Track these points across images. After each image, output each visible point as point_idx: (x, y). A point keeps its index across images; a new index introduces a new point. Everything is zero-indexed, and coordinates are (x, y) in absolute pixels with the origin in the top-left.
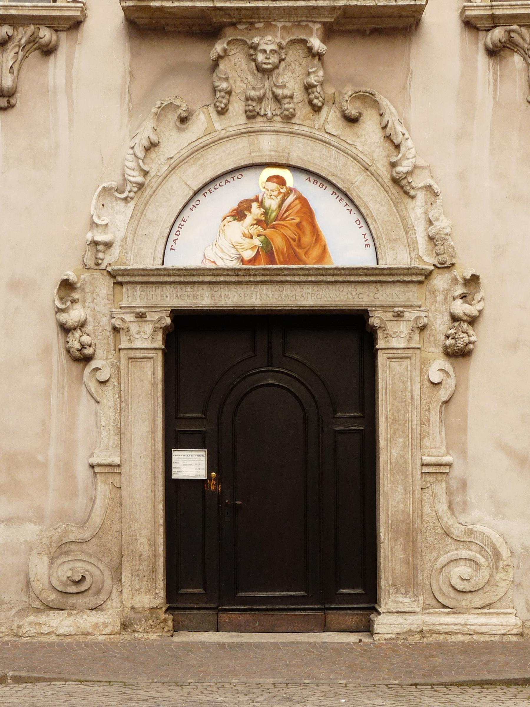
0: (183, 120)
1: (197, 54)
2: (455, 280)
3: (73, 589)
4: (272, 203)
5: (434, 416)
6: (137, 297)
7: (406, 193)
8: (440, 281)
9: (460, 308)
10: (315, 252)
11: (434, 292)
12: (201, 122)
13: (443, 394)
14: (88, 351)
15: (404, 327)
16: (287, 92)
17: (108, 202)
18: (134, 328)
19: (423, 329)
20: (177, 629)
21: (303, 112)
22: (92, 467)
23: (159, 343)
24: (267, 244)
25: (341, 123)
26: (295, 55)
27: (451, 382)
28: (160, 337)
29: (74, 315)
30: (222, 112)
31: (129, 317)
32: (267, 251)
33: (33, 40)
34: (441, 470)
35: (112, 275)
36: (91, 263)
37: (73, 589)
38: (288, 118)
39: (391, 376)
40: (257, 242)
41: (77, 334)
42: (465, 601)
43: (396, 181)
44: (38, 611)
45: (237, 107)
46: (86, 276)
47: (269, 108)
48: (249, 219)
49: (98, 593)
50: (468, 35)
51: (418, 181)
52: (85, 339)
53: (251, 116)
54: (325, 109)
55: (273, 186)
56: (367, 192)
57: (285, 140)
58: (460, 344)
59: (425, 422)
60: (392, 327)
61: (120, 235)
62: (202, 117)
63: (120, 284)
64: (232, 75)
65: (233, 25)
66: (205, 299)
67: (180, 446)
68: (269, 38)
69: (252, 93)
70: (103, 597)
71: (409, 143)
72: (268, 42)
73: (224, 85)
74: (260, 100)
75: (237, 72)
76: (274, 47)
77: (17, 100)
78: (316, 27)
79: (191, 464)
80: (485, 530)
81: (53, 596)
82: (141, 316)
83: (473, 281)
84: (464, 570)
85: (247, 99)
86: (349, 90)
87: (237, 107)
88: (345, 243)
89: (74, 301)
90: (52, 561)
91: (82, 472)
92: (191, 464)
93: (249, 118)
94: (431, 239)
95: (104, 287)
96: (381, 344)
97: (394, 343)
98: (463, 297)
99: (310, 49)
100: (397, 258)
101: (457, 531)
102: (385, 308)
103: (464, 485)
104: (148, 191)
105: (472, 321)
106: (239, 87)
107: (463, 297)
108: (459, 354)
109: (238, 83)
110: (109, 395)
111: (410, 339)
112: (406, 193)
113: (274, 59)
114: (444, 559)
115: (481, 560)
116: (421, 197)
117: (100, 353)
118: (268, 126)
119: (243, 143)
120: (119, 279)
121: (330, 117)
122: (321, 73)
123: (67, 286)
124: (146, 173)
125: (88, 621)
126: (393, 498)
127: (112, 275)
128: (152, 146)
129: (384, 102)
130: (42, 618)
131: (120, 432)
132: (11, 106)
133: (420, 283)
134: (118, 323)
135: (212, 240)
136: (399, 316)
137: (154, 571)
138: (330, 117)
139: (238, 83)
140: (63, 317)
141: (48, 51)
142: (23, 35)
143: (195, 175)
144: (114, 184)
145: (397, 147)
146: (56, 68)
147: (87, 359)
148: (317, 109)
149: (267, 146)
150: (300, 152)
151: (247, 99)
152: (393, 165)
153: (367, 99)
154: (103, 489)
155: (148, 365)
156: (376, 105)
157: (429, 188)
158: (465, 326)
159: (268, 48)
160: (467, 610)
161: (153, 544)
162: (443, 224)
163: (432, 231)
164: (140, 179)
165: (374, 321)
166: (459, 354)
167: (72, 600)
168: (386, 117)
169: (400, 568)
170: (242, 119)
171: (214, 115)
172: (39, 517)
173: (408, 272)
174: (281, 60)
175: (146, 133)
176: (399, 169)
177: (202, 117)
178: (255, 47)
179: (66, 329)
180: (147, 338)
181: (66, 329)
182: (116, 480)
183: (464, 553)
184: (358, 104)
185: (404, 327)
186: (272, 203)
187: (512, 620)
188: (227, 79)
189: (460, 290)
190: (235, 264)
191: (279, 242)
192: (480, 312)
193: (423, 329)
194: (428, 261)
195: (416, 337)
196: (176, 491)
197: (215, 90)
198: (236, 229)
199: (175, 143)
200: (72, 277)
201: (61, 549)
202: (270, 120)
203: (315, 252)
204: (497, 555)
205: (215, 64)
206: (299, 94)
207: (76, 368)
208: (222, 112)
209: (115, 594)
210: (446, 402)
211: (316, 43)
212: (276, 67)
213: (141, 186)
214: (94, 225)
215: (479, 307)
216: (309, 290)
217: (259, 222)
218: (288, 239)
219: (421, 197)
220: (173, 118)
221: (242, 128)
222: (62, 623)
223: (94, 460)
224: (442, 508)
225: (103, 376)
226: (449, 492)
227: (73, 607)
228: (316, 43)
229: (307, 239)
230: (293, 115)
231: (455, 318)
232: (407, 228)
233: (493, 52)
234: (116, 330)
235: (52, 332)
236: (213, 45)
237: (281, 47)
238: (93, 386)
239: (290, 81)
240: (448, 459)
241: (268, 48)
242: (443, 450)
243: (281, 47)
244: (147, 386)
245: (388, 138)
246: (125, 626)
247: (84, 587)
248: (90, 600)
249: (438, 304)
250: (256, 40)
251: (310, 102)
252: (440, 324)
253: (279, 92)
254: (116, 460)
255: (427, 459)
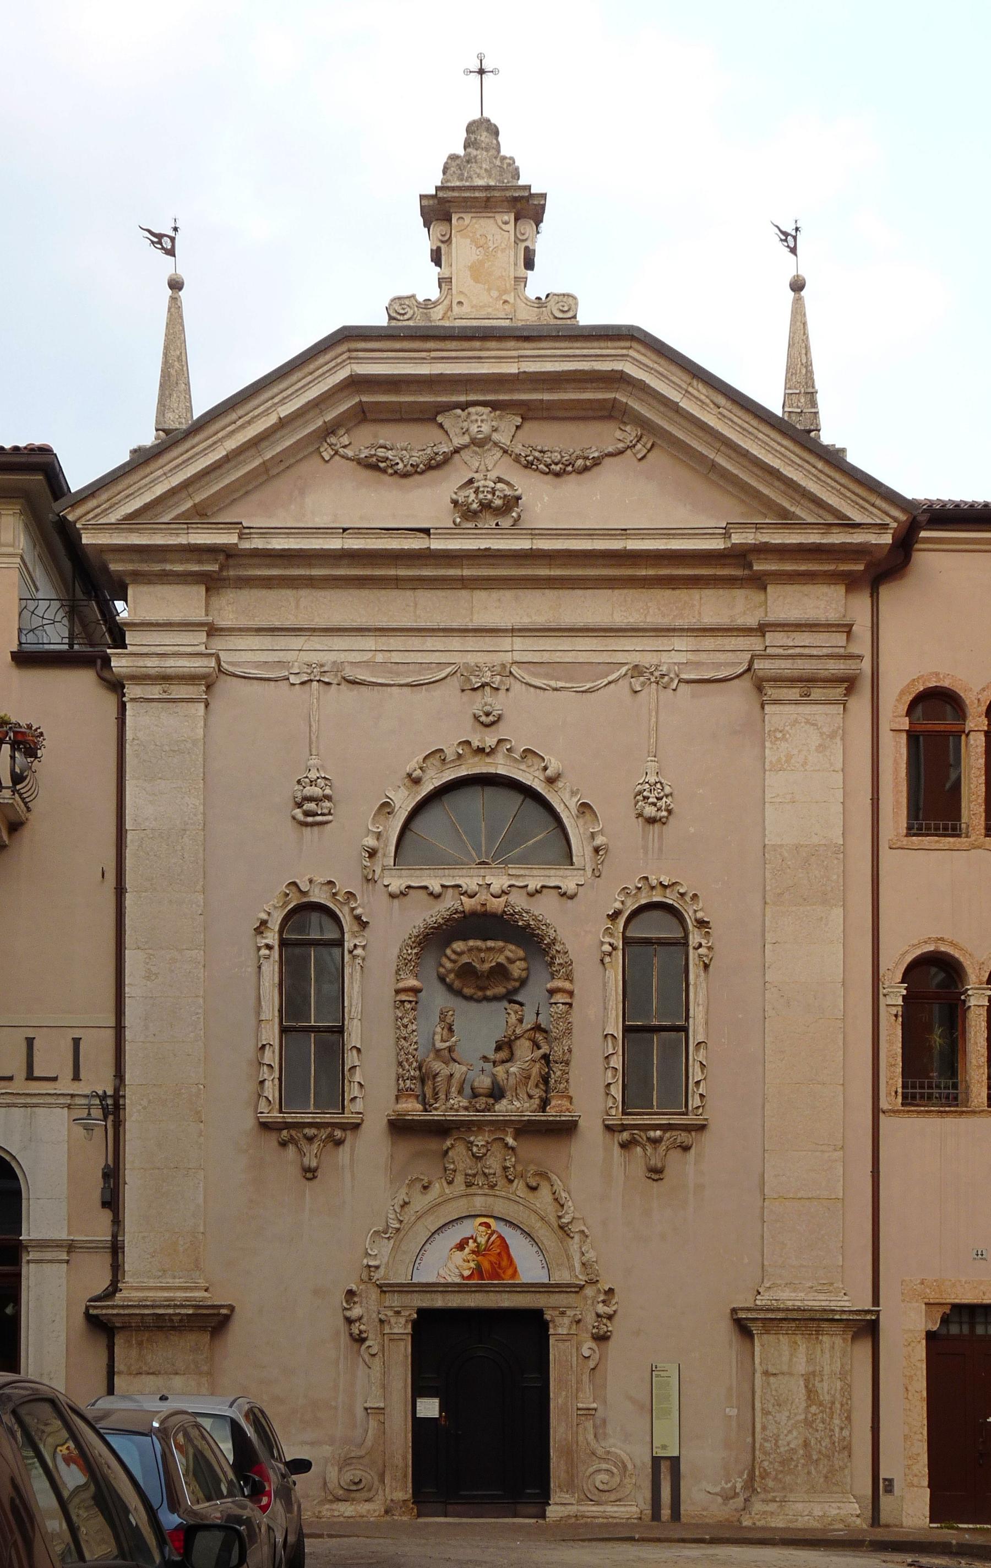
0: (425, 1188)
1: (433, 1145)
2: (599, 1290)
3: (354, 1488)
4: (482, 1240)
5: (585, 1378)
6: (395, 1300)
7: (568, 1235)
8: (589, 1291)
9: (601, 1309)
10: (510, 1272)
11: (585, 1298)
12: (436, 1188)
13: (592, 1364)
14: (364, 1335)
15: (566, 1321)
16: (492, 1171)
17: (377, 1239)
18: (393, 1320)
19: (578, 1322)
20: (419, 1516)
21: (502, 1182)
22: (366, 1409)
23: (409, 1330)
24: (479, 1266)
25: (526, 1189)
26: (496, 1147)
27: (597, 1356)
28: (410, 1326)
29: (356, 1312)
30: (450, 1183)
31: (390, 1313)
32: (478, 1272)
33: (330, 1136)
34: (589, 1413)
35: (380, 1286)
36: (365, 1277)
37: (354, 1488)
38: (492, 1187)
39: (559, 1353)
40: (472, 1265)
41: (357, 1324)
42: (604, 1497)
43: (561, 1227)
44: (331, 1502)
45: (459, 1179)
46: (362, 1287)
47: (480, 1180)
48: (467, 1250)
49: (370, 1490)
50: (608, 1135)
51: (575, 1228)
52: (362, 1327)
53: (469, 1185)
54: (516, 1181)
55: (482, 1228)
56: (542, 1233)
57: (490, 1200)
58: (602, 1333)
59: (579, 1382)
60: (559, 1320)
61: (385, 1260)
62: (437, 1185)
63: (385, 1292)
64: (456, 1158)
65: (458, 1128)
66: (439, 1302)
67: (422, 1396)
68: (480, 1138)
69: (470, 1172)
70: (373, 1492)
71: (570, 1203)
72: (480, 1140)
73: (452, 1166)
74: (474, 1176)
75: (459, 1154)
76: (483, 1143)
77: (319, 1173)
78: (510, 1130)
79: (429, 1408)
80: (618, 1451)
81: (341, 1492)
82: (398, 1313)
83: (610, 1291)
84: (603, 1477)
85: (466, 1175)
86: (532, 1168)
87: (459, 1179)
88: (529, 1266)
89: (355, 1303)
90: (340, 1470)
91: (360, 1413)
92: (429, 1408)
93: (467, 1186)
94: (584, 1264)
95: (374, 1294)
96: (551, 1331)
97: (560, 1331)
98: (604, 1302)
99: (507, 1144)
100: (562, 1276)
101: (600, 1452)
102: (554, 1308)
103: (604, 1421)
104: (403, 1233)
105: (610, 1317)
106: (461, 1166)
107: (604, 1302)
108: (602, 1339)
109: (461, 1164)
110: (377, 1363)
111: (570, 1328)
112: (568, 1235)
113: (483, 1150)
114: (591, 1470)
115: (615, 1470)
116: (577, 1237)
117: (371, 1336)
118: (480, 1192)
119: (464, 1201)
120: (384, 1289)
121: (519, 1186)
122: (513, 1159)
123: (351, 1293)
124: (401, 1222)
125: (364, 1508)
126: (558, 1431)
127: (380, 1286)
128: (405, 1204)
129: (554, 1177)
130: (334, 1506)
131: (384, 1387)
132: (315, 1177)
133: (577, 1292)
134: (383, 1317)
135: (444, 1266)
136: (563, 1313)
137: (405, 1476)
138: (519, 1186)
139: (461, 1164)
140: (348, 1314)
141: (339, 1143)
142: (324, 1134)
143: (433, 1223)
144: (381, 1229)
145: (562, 1206)
146: (343, 1154)
147: (363, 1340)
148: (511, 1181)
149: (479, 1203)
150: (500, 1207)
151: (466, 1175)
152: (560, 1217)
153: (543, 1175)
154: (373, 1424)
155: (402, 1343)
156: (549, 1179)
157: (583, 1232)
158: (605, 1321)
159: (480, 1144)
160: (606, 1503)
161: (405, 1458)
162: (591, 1255)
163: (584, 1259)
164: (397, 1226)
165: (547, 1317)
166: (602, 1339)
167: (353, 1495)
168: (555, 1187)
169: (563, 1475)
170: (463, 1187)
171: (445, 1184)
172: (332, 1442)
173: (569, 1286)
174: (488, 1150)
175: (402, 1196)
176: (563, 1220)
177: (437, 1185)
178: (472, 1143)
179: (349, 1321)
180: (401, 1327)
181: (349, 1321)
182: (381, 1417)
183: (604, 1466)
184: (537, 1178)
185: (566, 1321)
186: (482, 1240)
187: (634, 1509)
188: (453, 1163)
189: (602, 1297)
190: (458, 1280)
191: (486, 1265)
192: (615, 1312)
193: (578, 1322)
194: (582, 1279)
195: (574, 1327)
196: (419, 1425)
197: (445, 1169)
198: (459, 1256)
199: (420, 1202)
200: (354, 1288)
201: (345, 1462)
202: (481, 1188)
203: (510, 1272)
204: (625, 1466)
205: (446, 1152)
206: (499, 1171)
207: (356, 1346)
208: (450, 1183)
209: (380, 1492)
210: (593, 1369)
211: (510, 1141)
212: (485, 1155)
213: (398, 1230)
214: (367, 1255)
215: (614, 1308)
216: (505, 1296)
217: (473, 1252)
218: (493, 1263)
219: (577, 1237)
220: (418, 1186)
221: (463, 1193)
222: (347, 1509)
223: (367, 1405)
224: (591, 1437)
225: (373, 1351)
226: (595, 1427)
227: (353, 1500)
228: (510, 1141)
229: (505, 1263)
230: (496, 1185)
231: (598, 1316)
232: (569, 1257)
233: (624, 1146)
234: (381, 1321)
235: (341, 1322)
236: (446, 1140)
237: (488, 1143)
238: (366, 1357)
239: (494, 1163)
240: (595, 1405)
241: (480, 1144)
242: (591, 1399)
243: (488, 1143)
244: (401, 1357)
245: (556, 1200)
246: (387, 1512)
247: (361, 1486)
248: (364, 1495)
249: (589, 1307)
250: (472, 1139)
251: (507, 1177)
252: (590, 1319)
253: (487, 1171)
254: (382, 1405)
255: (580, 1405)
